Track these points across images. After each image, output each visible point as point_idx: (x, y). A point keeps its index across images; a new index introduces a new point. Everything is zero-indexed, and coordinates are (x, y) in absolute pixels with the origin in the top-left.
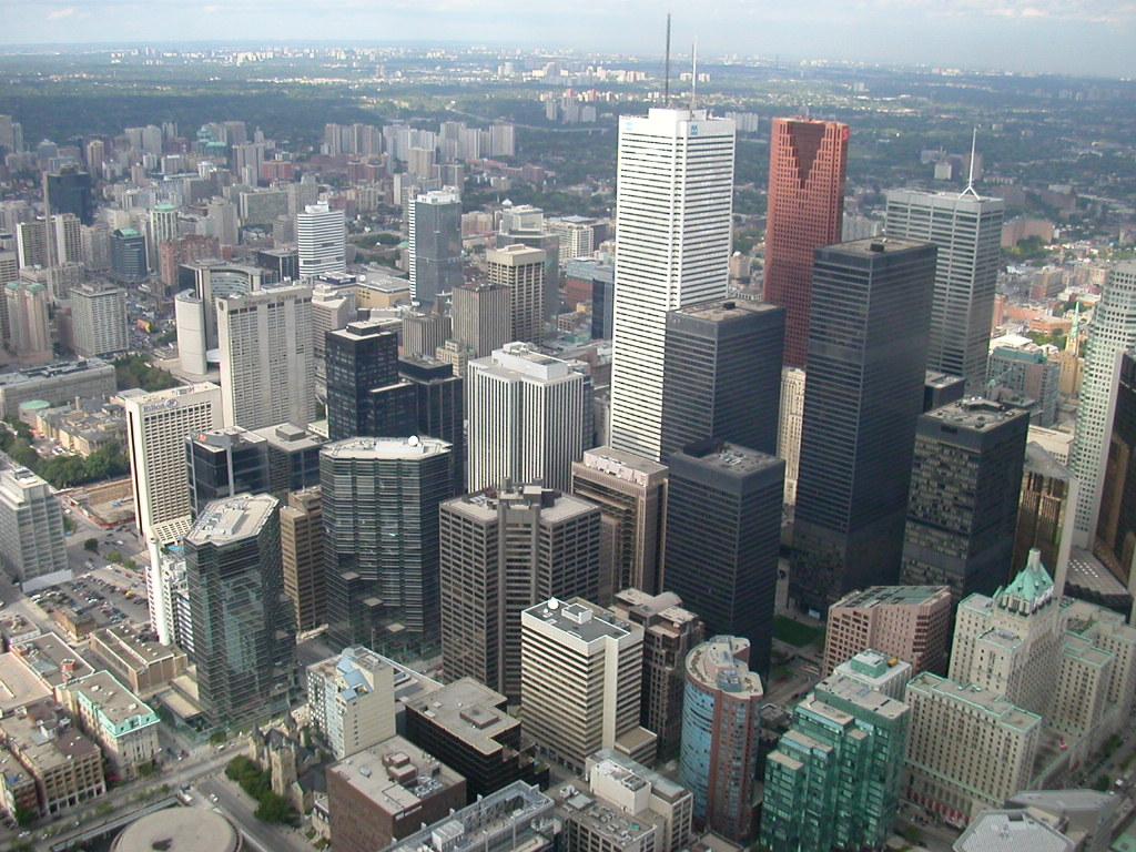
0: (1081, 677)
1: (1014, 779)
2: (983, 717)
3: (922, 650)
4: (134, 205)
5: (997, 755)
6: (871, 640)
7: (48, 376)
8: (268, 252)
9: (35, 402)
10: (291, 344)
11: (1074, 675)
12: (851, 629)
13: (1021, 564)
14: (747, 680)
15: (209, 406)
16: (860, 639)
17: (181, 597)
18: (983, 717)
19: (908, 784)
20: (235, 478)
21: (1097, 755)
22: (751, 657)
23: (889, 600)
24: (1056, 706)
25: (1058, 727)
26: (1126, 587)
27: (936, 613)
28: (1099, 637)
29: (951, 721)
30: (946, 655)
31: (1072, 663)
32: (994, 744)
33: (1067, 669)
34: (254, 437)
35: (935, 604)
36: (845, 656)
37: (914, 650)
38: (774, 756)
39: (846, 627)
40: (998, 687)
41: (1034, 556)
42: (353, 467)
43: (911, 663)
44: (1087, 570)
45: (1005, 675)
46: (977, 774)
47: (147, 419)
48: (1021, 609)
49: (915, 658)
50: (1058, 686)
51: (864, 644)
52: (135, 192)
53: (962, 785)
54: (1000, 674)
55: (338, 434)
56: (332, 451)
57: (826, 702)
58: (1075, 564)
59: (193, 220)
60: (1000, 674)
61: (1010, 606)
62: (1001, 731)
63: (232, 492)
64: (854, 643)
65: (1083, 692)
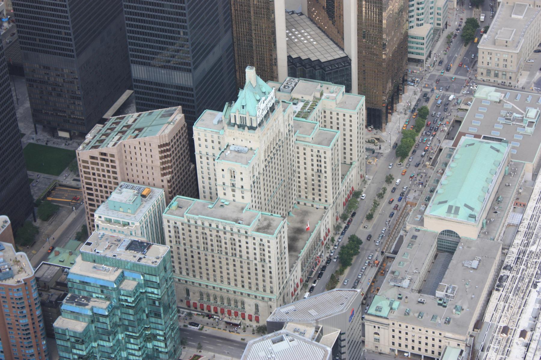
0: (315, 158)
3: (169, 173)
5: (255, 259)
11: (309, 158)
12: (100, 167)
13: (241, 84)
14: (17, 262)
18: (235, 230)
19: (186, 296)
21: (344, 217)
22: (15, 235)
23: (129, 132)
25: (305, 204)
26: (343, 49)
27: (176, 137)
28: (325, 112)
29: (209, 238)
30: (193, 166)
31: (304, 149)
32: (251, 250)
36: (102, 197)
38: (60, 323)
39: (95, 167)
40: (243, 197)
41: (250, 73)
43: (163, 186)
45: (247, 187)
48: (248, 124)
49: (165, 183)
50: (297, 170)
51: (116, 178)
53: (232, 288)
57: (94, 261)
61: (238, 122)
62: (254, 239)
64: (107, 179)
65: (319, 171)
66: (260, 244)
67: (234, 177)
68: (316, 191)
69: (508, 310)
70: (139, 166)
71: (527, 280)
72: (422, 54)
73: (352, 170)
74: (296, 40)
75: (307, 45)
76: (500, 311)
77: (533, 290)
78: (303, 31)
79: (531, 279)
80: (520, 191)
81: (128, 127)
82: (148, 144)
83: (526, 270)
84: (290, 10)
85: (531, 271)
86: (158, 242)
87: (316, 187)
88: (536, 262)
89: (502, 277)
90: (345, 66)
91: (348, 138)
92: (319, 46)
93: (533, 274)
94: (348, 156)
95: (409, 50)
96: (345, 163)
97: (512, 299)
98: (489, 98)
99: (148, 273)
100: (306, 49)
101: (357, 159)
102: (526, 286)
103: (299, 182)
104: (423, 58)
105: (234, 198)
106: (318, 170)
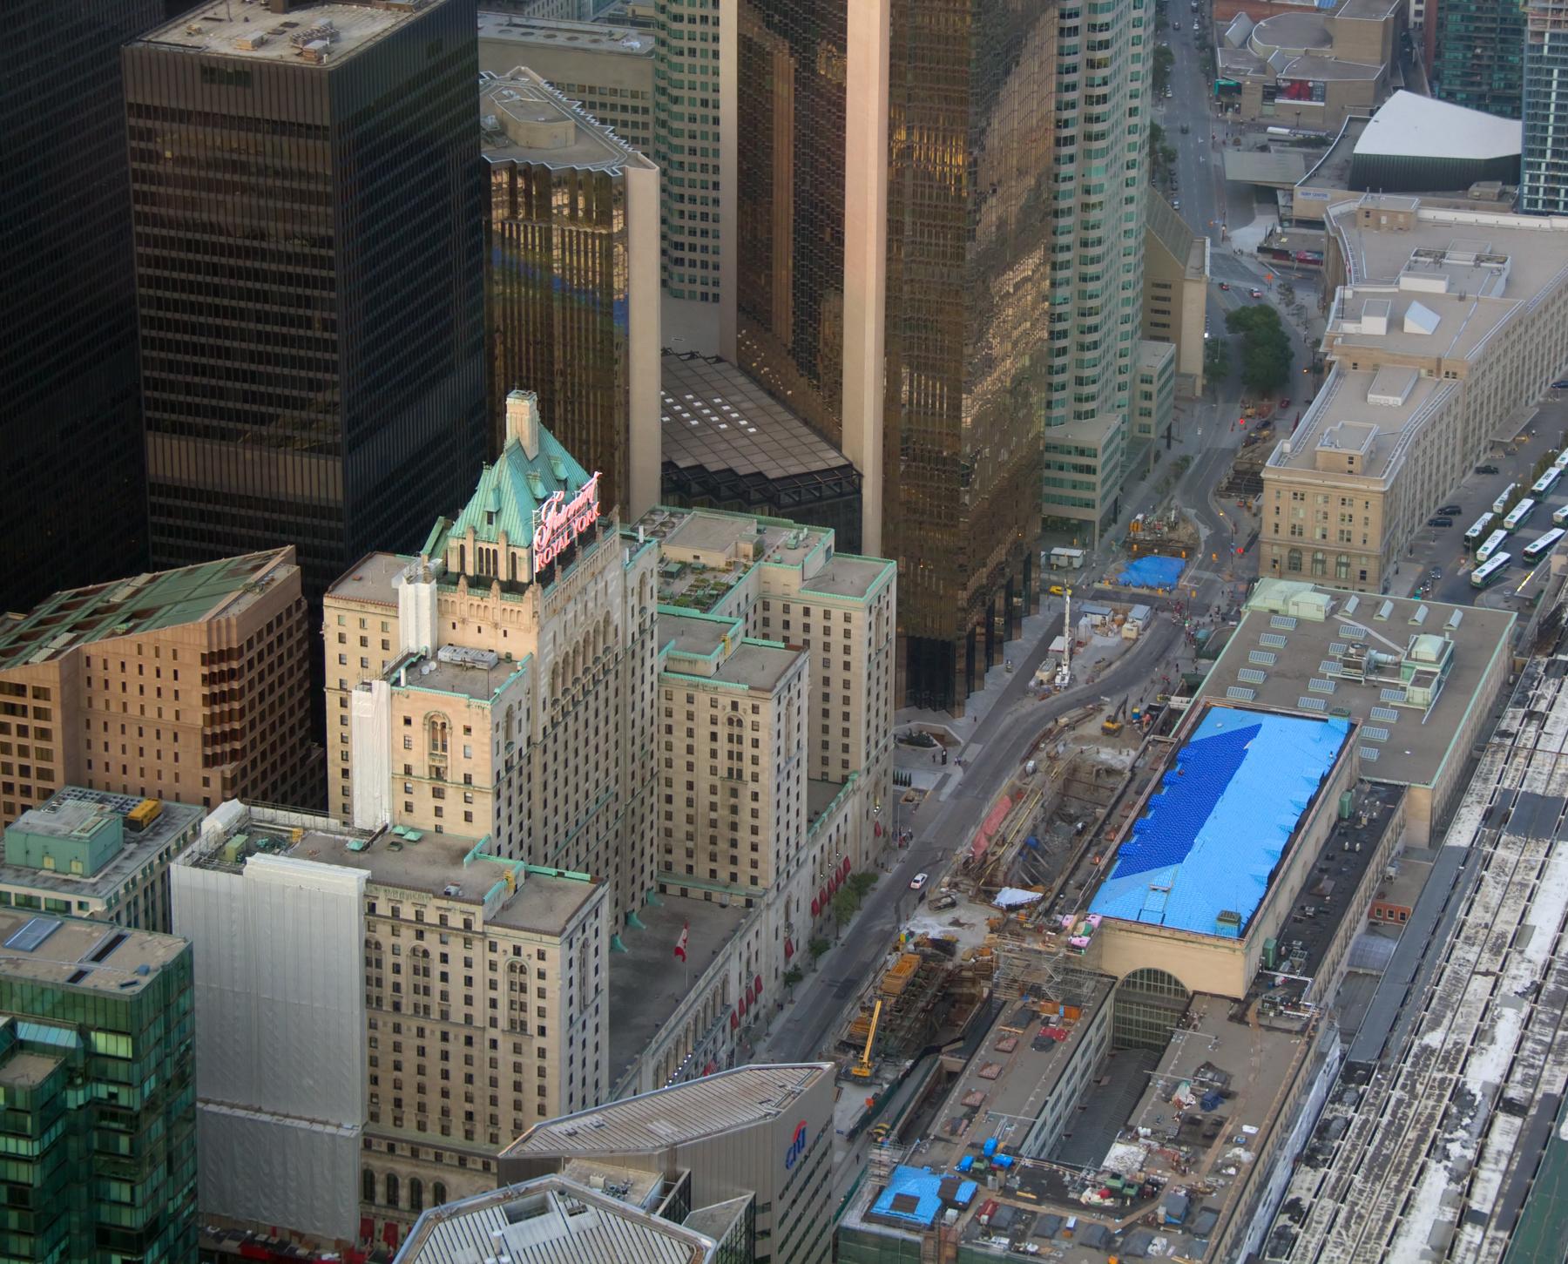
0: (723, 731)
1: (553, 1082)
2: (431, 917)
3: (234, 755)
6: (71, 760)
11: (703, 732)
16: (33, 763)
24: (669, 833)
28: (766, 606)
31: (690, 700)
33: (679, 716)
35: (258, 606)
37: (210, 761)
40: (468, 817)
44: (724, 417)
45: (484, 779)
46: (445, 1094)
50: (665, 772)
54: (468, 779)
58: (688, 407)
60: (468, 779)
62: (493, 947)
65: (735, 775)
66: (512, 967)
67: (444, 748)
68: (723, 845)
69: (1347, 1226)
70: (132, 731)
71: (1412, 1135)
72: (1089, 504)
73: (847, 798)
74: (694, 423)
75: (727, 437)
76: (1321, 1228)
77: (1432, 1164)
78: (718, 400)
79: (1425, 1131)
80: (1391, 871)
81: (112, 608)
82: (166, 654)
83: (1410, 1105)
84: (682, 347)
85: (1425, 1105)
86: (152, 927)
87: (724, 831)
88: (1443, 1080)
89: (1328, 1123)
90: (841, 495)
91: (836, 689)
92: (765, 438)
93: (1431, 1117)
94: (835, 753)
95: (1048, 490)
96: (824, 779)
97: (1361, 1192)
98: (1293, 611)
99: (101, 1022)
100: (724, 446)
101: (863, 765)
102: (1409, 1151)
103: (669, 816)
104: (1095, 515)
105: (438, 821)
106: (730, 770)
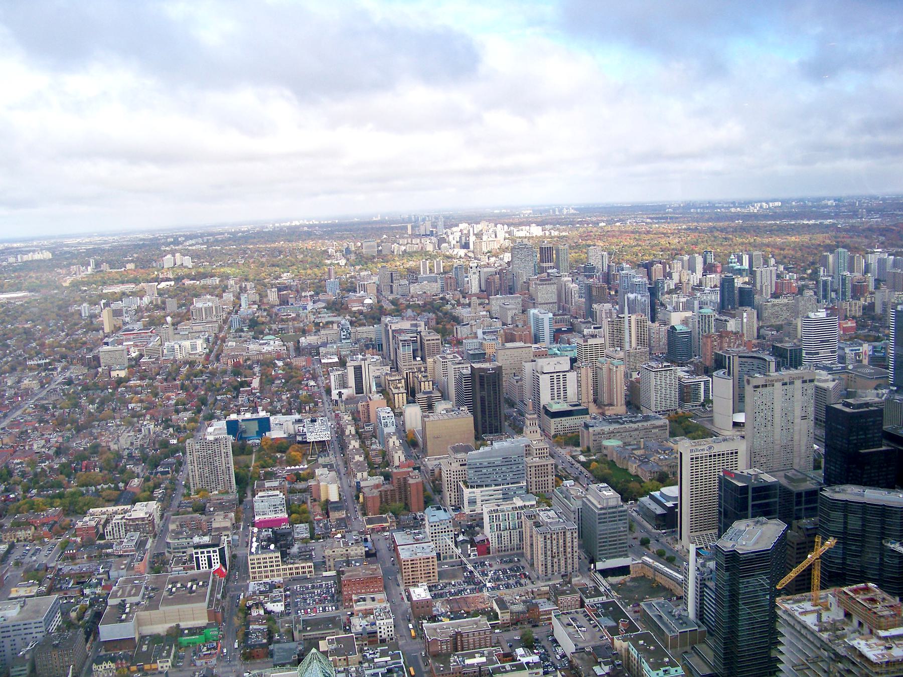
4: (684, 310)
7: (622, 424)
8: (779, 345)
9: (612, 440)
10: (798, 413)
15: (736, 453)
17: (706, 586)
20: (753, 505)
34: (769, 479)
42: (846, 506)
47: (692, 459)
52: (684, 300)
55: (830, 481)
56: (828, 493)
59: (726, 321)
63: (750, 515)
